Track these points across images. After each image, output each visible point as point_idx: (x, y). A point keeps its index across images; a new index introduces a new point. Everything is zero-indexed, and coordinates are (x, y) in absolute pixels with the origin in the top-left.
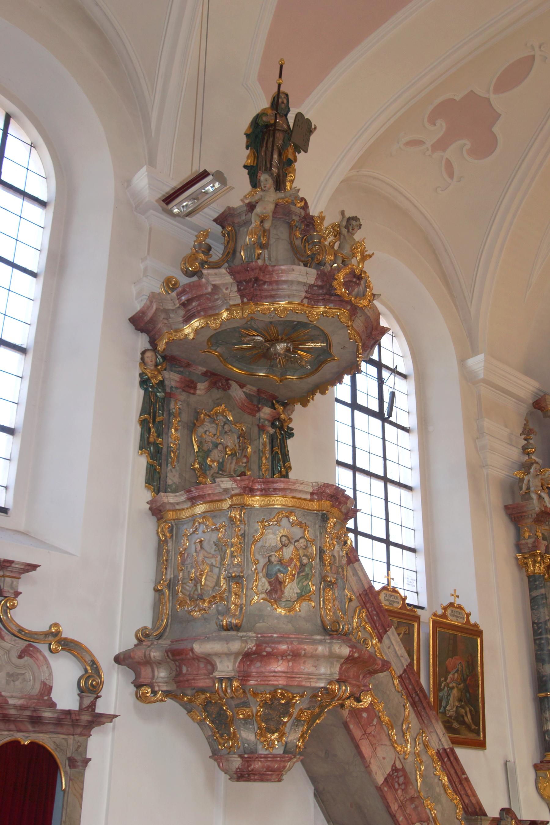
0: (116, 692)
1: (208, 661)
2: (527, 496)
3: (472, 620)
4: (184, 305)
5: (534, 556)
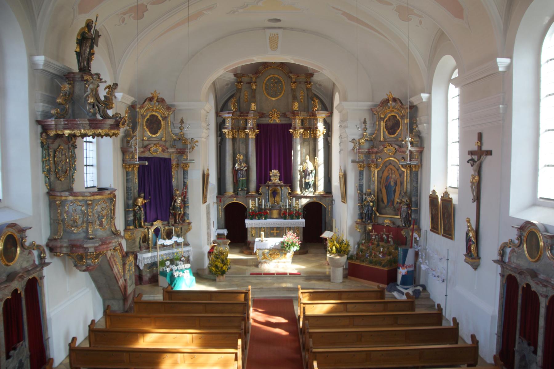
2: (131, 147)
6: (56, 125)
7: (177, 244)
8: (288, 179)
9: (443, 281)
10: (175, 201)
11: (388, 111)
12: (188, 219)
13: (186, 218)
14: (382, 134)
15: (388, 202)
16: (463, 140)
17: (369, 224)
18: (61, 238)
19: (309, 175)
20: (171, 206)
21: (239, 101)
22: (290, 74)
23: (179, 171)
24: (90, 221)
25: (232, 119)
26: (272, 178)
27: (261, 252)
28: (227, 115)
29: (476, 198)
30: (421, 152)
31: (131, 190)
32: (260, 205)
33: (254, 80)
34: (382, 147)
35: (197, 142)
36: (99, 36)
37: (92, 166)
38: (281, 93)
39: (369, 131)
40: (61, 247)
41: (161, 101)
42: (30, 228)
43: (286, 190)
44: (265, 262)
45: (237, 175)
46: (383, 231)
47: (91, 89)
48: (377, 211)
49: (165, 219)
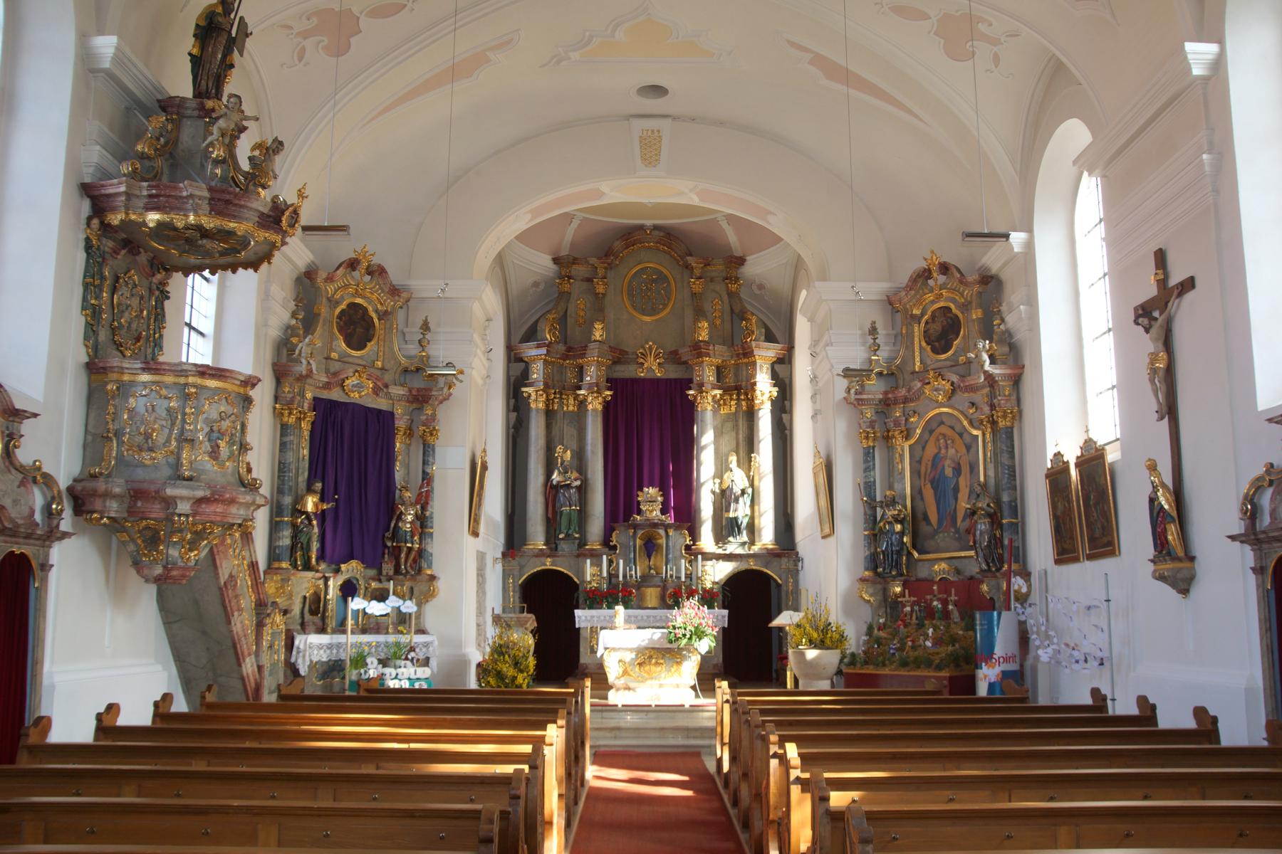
2: (298, 361)
4: (150, 196)
5: (290, 409)
6: (128, 195)
7: (402, 619)
9: (1102, 664)
10: (399, 518)
12: (430, 567)
13: (424, 565)
14: (917, 354)
15: (940, 522)
16: (1119, 274)
17: (894, 577)
18: (109, 476)
19: (737, 501)
20: (388, 530)
21: (563, 319)
23: (412, 448)
24: (188, 435)
25: (546, 363)
26: (643, 508)
28: (534, 352)
29: (1165, 409)
30: (1016, 381)
31: (289, 471)
33: (601, 272)
34: (919, 385)
36: (247, 35)
37: (202, 334)
38: (665, 306)
39: (883, 354)
40: (107, 495)
41: (377, 272)
42: (35, 415)
43: (680, 539)
46: (932, 592)
47: (220, 129)
48: (914, 547)
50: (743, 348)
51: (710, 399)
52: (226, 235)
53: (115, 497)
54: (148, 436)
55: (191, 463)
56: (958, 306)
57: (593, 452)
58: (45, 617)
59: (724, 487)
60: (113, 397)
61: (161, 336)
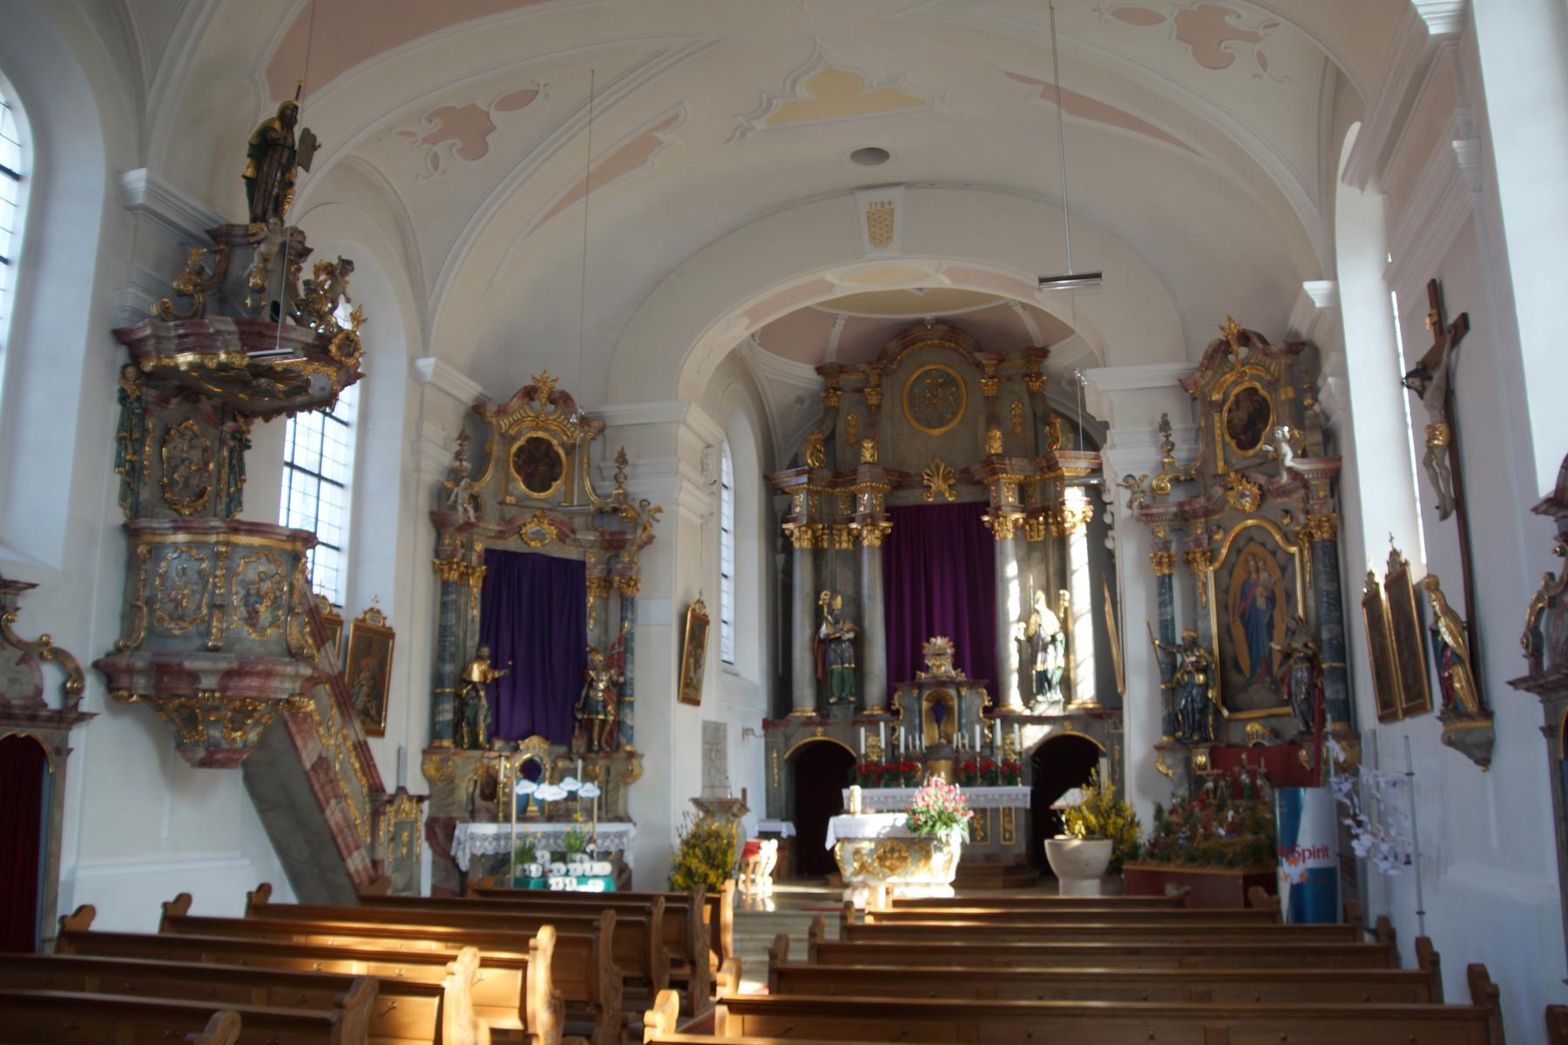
0: (92, 696)
1: (194, 676)
2: (453, 508)
3: (388, 623)
4: (181, 337)
5: (450, 563)
8: (981, 661)
10: (591, 684)
11: (1230, 378)
12: (630, 740)
13: (623, 740)
17: (1197, 744)
18: (138, 648)
19: (1045, 649)
20: (578, 699)
21: (830, 439)
22: (978, 355)
25: (810, 493)
26: (929, 662)
27: (850, 847)
28: (794, 481)
29: (1449, 503)
32: (893, 746)
35: (659, 510)
36: (315, 147)
38: (955, 414)
39: (1181, 453)
41: (562, 400)
42: (33, 586)
44: (864, 885)
45: (825, 653)
46: (1239, 762)
48: (1224, 703)
49: (557, 735)
50: (1048, 460)
51: (1010, 525)
52: (258, 371)
53: (139, 672)
54: (178, 603)
55: (222, 630)
56: (1264, 387)
57: (870, 598)
58: (61, 806)
59: (1032, 631)
60: (144, 561)
61: (240, 491)
